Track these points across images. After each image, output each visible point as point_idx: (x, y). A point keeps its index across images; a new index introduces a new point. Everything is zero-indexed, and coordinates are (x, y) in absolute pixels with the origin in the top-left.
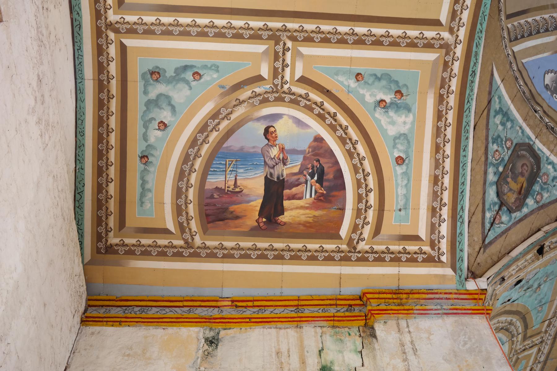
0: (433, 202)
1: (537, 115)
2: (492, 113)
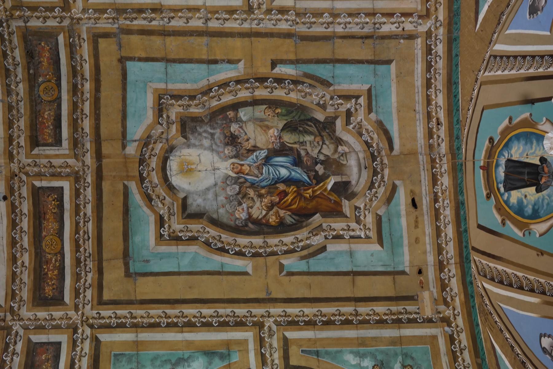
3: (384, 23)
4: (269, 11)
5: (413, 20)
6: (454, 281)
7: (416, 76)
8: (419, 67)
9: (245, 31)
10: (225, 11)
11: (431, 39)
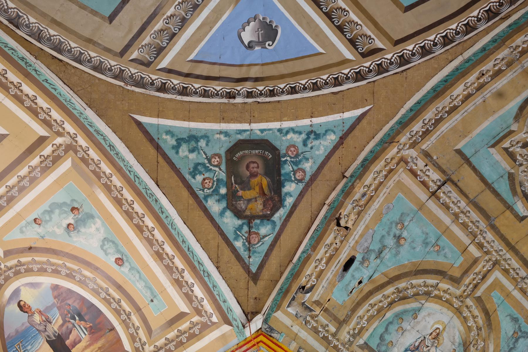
0: (172, 275)
1: (239, 100)
2: (171, 154)
3: (433, 181)
4: (487, 253)
5: (413, 165)
7: (454, 124)
8: (444, 128)
9: (512, 253)
10: (508, 275)
11: (415, 140)
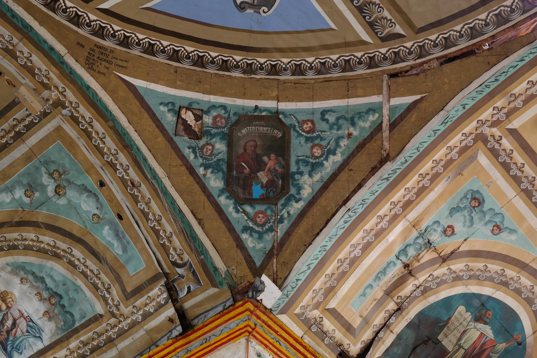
6: (35, 58)
